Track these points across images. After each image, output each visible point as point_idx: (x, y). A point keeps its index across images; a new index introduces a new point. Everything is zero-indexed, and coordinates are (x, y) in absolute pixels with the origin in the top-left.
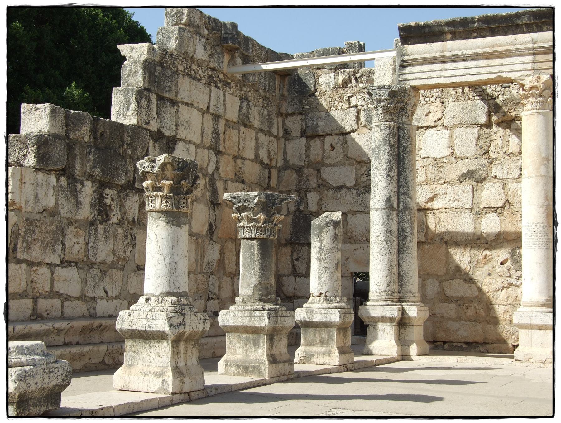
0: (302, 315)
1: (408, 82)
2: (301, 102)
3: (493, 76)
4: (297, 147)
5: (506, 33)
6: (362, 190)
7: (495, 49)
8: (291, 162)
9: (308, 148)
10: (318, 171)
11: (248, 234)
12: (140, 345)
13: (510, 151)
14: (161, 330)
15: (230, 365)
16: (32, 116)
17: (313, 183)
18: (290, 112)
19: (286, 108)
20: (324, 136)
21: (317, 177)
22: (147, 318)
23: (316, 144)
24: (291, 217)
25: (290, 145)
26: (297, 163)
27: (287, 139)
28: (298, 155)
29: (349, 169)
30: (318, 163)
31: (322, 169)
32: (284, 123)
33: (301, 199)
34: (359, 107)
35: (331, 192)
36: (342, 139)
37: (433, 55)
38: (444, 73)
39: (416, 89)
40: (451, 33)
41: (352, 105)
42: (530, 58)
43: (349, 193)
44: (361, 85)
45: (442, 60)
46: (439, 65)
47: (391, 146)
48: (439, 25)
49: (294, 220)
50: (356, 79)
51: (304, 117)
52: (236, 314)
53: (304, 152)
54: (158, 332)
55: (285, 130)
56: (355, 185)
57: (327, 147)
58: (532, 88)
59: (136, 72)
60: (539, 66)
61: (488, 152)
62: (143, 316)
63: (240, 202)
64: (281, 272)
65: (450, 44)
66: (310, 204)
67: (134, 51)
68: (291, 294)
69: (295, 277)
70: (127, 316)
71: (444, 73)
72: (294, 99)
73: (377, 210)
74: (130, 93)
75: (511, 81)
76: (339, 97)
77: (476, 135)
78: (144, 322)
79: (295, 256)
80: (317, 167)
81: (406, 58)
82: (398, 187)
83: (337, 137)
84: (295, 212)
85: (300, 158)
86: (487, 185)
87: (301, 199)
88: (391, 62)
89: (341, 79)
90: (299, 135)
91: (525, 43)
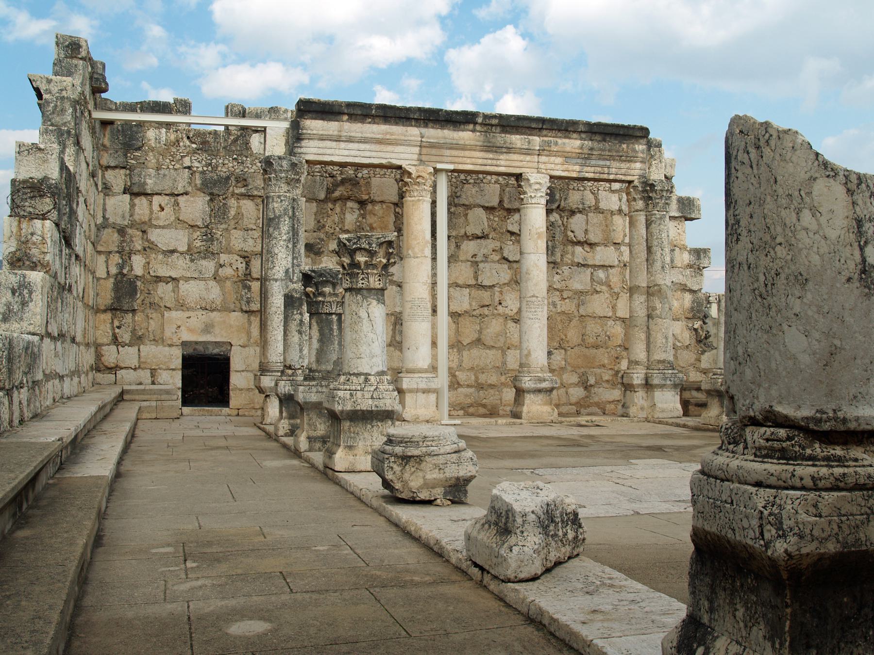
0: (287, 388)
1: (303, 156)
2: (125, 156)
3: (384, 162)
4: (118, 206)
5: (397, 124)
6: (196, 255)
7: (388, 137)
8: (111, 220)
9: (132, 206)
11: (326, 310)
12: (360, 425)
13: (346, 228)
14: (390, 409)
15: (315, 441)
16: (31, 158)
17: (138, 245)
18: (113, 164)
19: (106, 160)
20: (152, 195)
21: (142, 238)
22: (372, 398)
23: (141, 202)
24: (112, 280)
25: (111, 202)
26: (119, 221)
27: (106, 195)
28: (121, 213)
29: (181, 232)
30: (144, 223)
31: (149, 231)
32: (103, 176)
33: (124, 262)
34: (195, 169)
35: (160, 257)
36: (173, 200)
37: (331, 133)
38: (337, 152)
39: (307, 161)
40: (348, 114)
41: (185, 165)
43: (181, 258)
44: (194, 146)
45: (338, 140)
46: (334, 143)
47: (290, 218)
48: (340, 104)
49: (116, 284)
50: (188, 138)
51: (128, 172)
52: (320, 390)
53: (128, 210)
54: (388, 411)
55: (105, 184)
56: (188, 250)
57: (156, 208)
58: (419, 176)
59: (63, 111)
60: (424, 158)
61: (324, 226)
62: (368, 395)
64: (99, 341)
65: (347, 126)
66: (135, 267)
67: (52, 84)
68: (113, 365)
69: (117, 346)
70: (348, 397)
71: (337, 152)
72: (117, 152)
73: (276, 280)
74: (65, 136)
75: (399, 167)
76: (171, 156)
77: (315, 210)
78: (370, 402)
79: (116, 323)
80: (144, 228)
81: (304, 131)
82: (293, 259)
83: (167, 198)
84: (117, 275)
85: (123, 217)
87: (124, 262)
89: (173, 137)
90: (122, 190)
91: (414, 136)
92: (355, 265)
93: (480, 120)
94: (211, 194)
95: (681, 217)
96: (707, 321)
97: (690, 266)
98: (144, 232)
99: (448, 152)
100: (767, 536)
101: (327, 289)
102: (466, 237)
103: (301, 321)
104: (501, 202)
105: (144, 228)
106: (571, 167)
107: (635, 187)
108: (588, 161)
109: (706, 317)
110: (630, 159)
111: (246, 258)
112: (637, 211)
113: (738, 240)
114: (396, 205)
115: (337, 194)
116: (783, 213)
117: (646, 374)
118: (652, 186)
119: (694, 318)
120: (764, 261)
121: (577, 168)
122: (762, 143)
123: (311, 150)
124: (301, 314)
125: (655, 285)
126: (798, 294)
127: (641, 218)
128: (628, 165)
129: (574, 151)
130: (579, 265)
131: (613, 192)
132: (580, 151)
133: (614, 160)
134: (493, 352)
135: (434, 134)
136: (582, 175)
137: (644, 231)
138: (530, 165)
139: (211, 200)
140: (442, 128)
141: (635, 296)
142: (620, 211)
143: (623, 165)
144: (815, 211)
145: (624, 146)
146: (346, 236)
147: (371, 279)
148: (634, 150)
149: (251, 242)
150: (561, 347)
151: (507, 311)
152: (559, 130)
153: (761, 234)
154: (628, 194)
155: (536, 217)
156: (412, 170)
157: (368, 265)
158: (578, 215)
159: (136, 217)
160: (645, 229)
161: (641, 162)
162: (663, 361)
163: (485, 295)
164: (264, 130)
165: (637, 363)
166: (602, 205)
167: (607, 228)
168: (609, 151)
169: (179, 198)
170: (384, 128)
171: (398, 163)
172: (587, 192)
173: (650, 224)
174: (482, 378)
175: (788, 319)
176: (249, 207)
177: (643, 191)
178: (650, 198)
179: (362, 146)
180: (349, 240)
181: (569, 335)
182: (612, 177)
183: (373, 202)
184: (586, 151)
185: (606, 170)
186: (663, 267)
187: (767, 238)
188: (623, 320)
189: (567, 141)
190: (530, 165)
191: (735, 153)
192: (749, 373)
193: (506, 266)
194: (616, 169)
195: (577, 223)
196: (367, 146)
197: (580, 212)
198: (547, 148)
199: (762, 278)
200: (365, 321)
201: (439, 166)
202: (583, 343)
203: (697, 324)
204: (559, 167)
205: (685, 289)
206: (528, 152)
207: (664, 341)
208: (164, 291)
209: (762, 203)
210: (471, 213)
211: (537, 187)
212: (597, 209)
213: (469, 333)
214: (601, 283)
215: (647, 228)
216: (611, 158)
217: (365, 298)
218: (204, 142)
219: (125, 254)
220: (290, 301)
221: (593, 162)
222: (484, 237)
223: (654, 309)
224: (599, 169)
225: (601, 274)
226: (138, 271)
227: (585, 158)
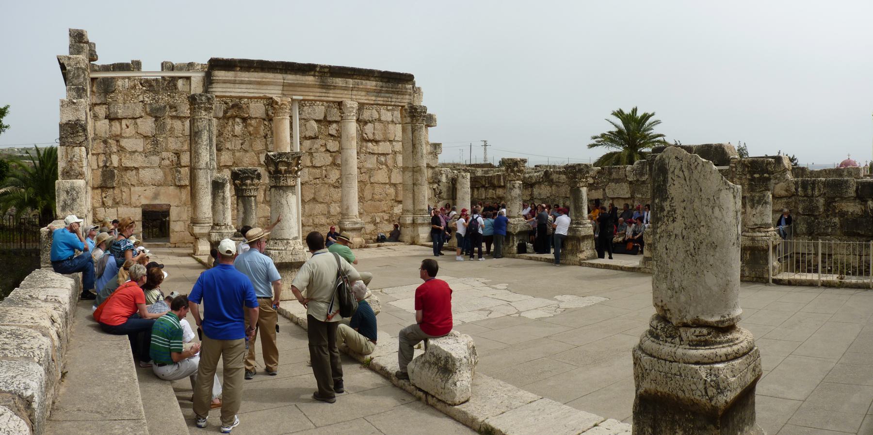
4: (103, 125)
5: (269, 72)
9: (111, 126)
10: (118, 141)
11: (248, 194)
20: (121, 119)
23: (116, 124)
31: (121, 140)
42: (281, 88)
45: (234, 82)
57: (124, 126)
60: (285, 93)
63: (245, 173)
65: (239, 74)
75: (271, 98)
80: (117, 138)
86: (223, 153)
88: (200, 79)
92: (277, 171)
93: (318, 69)
94: (156, 117)
97: (431, 153)
98: (118, 141)
99: (299, 89)
100: (710, 393)
101: (249, 182)
102: (306, 138)
103: (224, 198)
104: (325, 117)
105: (117, 138)
107: (406, 110)
109: (439, 181)
110: (403, 94)
111: (178, 154)
113: (674, 221)
114: (264, 120)
115: (229, 114)
116: (705, 208)
118: (416, 109)
119: (434, 182)
120: (693, 235)
121: (374, 98)
122: (693, 167)
123: (218, 90)
124: (224, 192)
126: (712, 253)
127: (409, 128)
130: (370, 153)
131: (388, 110)
134: (323, 205)
135: (291, 78)
137: (410, 135)
139: (156, 120)
140: (296, 74)
141: (406, 173)
142: (393, 121)
144: (721, 208)
146: (272, 153)
147: (289, 181)
149: (179, 144)
151: (330, 181)
152: (364, 76)
153: (692, 220)
154: (401, 113)
155: (352, 127)
156: (278, 99)
157: (286, 172)
158: (369, 124)
159: (113, 133)
163: (318, 171)
164: (188, 78)
165: (408, 211)
166: (383, 118)
167: (385, 132)
169: (138, 120)
170: (261, 74)
171: (270, 96)
172: (374, 111)
174: (317, 221)
175: (707, 268)
176: (177, 124)
178: (414, 116)
179: (249, 86)
180: (274, 156)
181: (365, 194)
183: (251, 118)
187: (695, 222)
188: (395, 185)
191: (672, 169)
192: (683, 298)
193: (328, 154)
194: (395, 99)
195: (369, 128)
196: (252, 86)
199: (692, 245)
200: (285, 206)
201: (294, 97)
202: (373, 199)
203: (435, 186)
205: (428, 166)
206: (345, 88)
208: (130, 176)
209: (692, 202)
210: (308, 124)
212: (379, 120)
213: (309, 196)
214: (382, 164)
216: (393, 92)
217: (285, 191)
218: (150, 85)
219: (108, 155)
220: (217, 186)
222: (316, 138)
223: (417, 180)
225: (383, 159)
226: (116, 164)
227: (378, 92)
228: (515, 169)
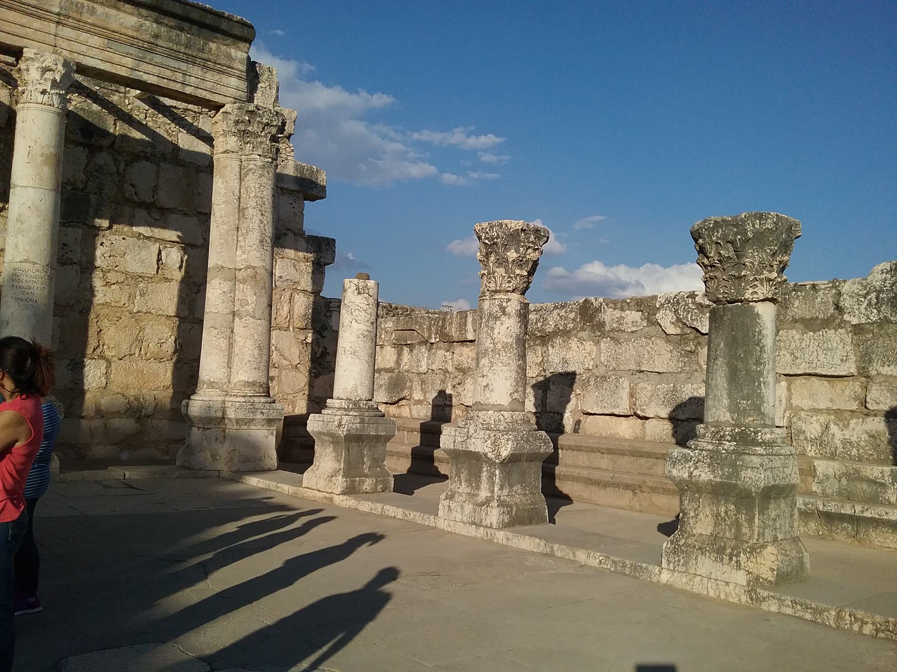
95: (298, 192)
96: (324, 334)
106: (117, 58)
108: (149, 56)
112: (226, 152)
117: (224, 402)
121: (129, 62)
125: (247, 268)
128: (217, 77)
129: (123, 31)
132: (135, 34)
133: (194, 63)
136: (136, 75)
138: (40, 36)
143: (209, 75)
145: (213, 45)
148: (229, 57)
150: (102, 357)
158: (144, 164)
160: (237, 181)
161: (239, 77)
162: (253, 384)
165: (211, 385)
168: (187, 46)
173: (246, 174)
177: (237, 122)
182: (188, 90)
184: (147, 37)
185: (179, 77)
186: (261, 241)
189: (113, 12)
190: (40, 36)
197: (147, 159)
198: (75, 15)
204: (94, 52)
207: (256, 352)
211: (48, 75)
215: (241, 180)
216: (191, 60)
221: (158, 59)
224: (168, 73)
228: (512, 255)
